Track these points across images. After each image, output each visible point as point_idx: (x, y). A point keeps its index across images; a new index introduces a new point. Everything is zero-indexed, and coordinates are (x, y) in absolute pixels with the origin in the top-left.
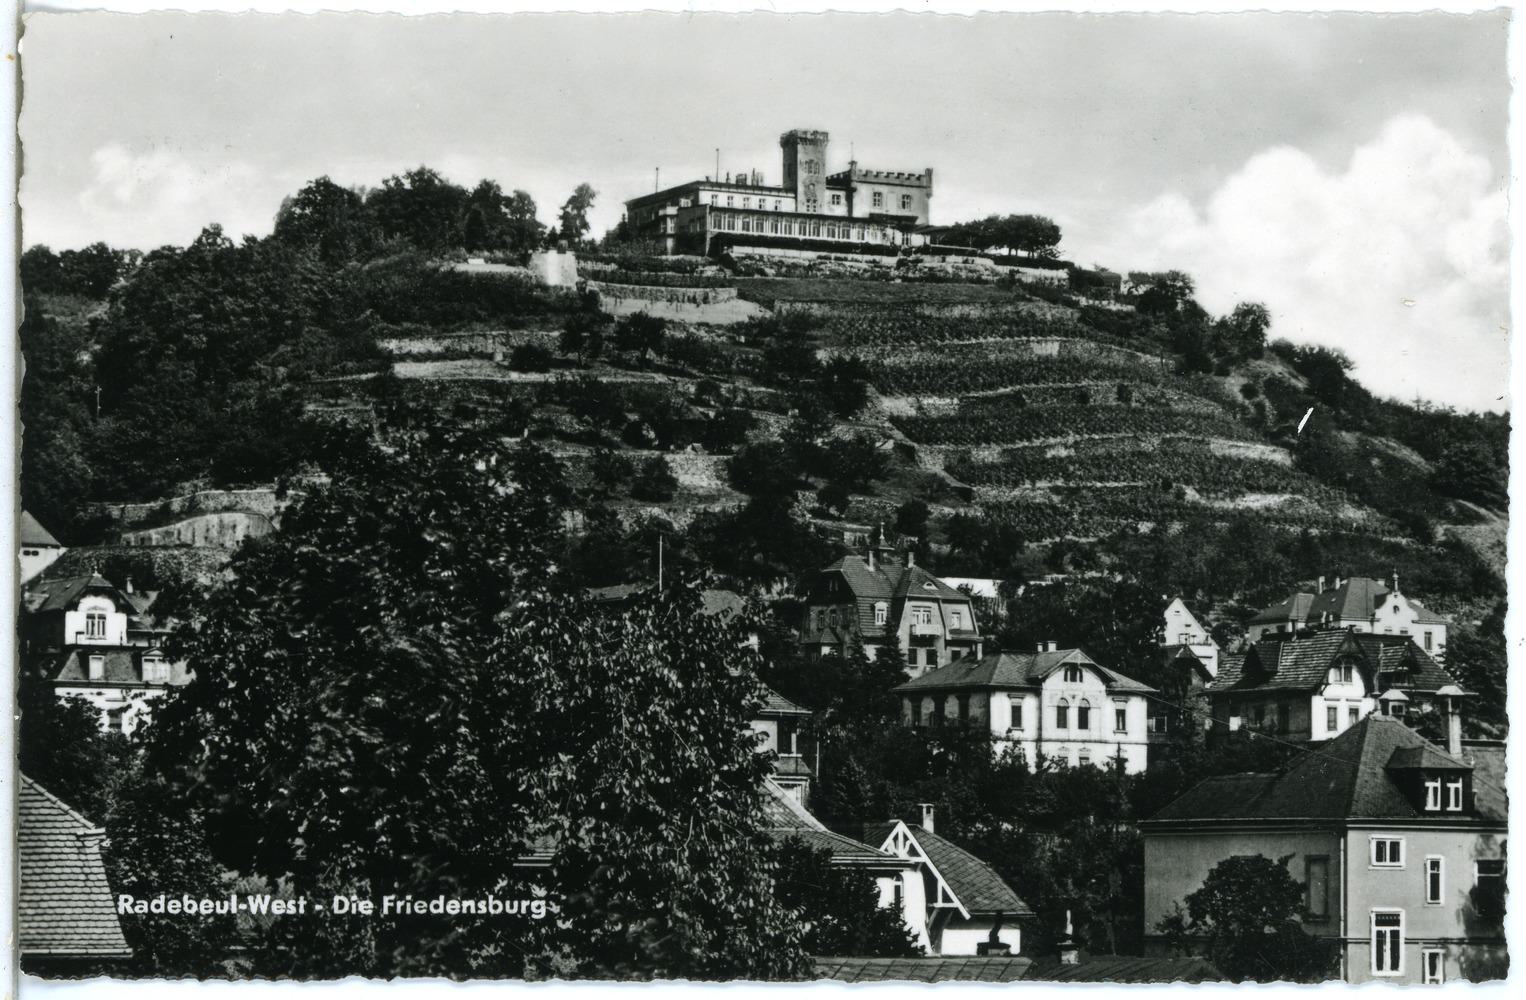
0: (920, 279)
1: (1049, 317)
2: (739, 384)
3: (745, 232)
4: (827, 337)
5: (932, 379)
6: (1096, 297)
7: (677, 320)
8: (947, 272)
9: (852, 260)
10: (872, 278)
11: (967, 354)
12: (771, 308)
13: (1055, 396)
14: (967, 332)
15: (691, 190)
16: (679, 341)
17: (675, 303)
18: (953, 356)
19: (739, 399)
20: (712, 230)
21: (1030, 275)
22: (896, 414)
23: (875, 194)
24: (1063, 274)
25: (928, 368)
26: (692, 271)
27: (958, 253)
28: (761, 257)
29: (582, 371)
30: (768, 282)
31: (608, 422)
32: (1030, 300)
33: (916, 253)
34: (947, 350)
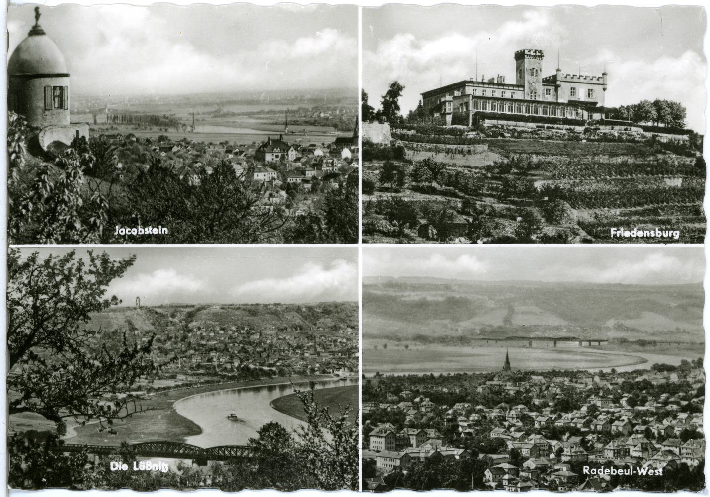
0: (598, 140)
1: (676, 163)
5: (604, 199)
8: (614, 136)
9: (558, 128)
10: (569, 140)
11: (625, 185)
12: (508, 157)
13: (679, 211)
14: (626, 172)
15: (461, 85)
17: (450, 154)
18: (617, 186)
19: (488, 211)
20: (472, 110)
21: (665, 138)
22: (581, 221)
23: (572, 89)
24: (686, 137)
25: (602, 193)
26: (461, 135)
28: (503, 126)
29: (393, 194)
30: (506, 141)
31: (408, 224)
32: (665, 153)
33: (595, 124)
34: (613, 183)
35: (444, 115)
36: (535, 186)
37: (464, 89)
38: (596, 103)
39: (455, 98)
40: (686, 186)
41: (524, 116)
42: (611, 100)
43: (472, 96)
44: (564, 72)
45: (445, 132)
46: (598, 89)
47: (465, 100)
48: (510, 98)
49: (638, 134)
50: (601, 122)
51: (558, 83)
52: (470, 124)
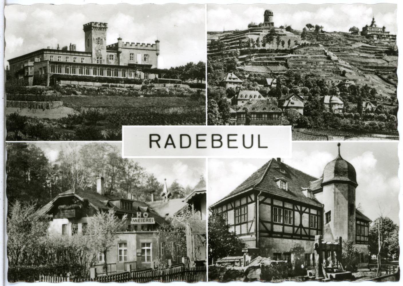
3: (66, 74)
4: (106, 124)
7: (33, 117)
8: (166, 92)
9: (120, 87)
10: (129, 95)
12: (79, 111)
15: (40, 53)
16: (33, 128)
17: (32, 110)
23: (131, 54)
26: (41, 93)
27: (172, 82)
28: (75, 85)
30: (78, 98)
33: (151, 82)
35: (27, 77)
36: (102, 134)
37: (43, 56)
38: (151, 66)
39: (35, 63)
43: (50, 62)
44: (125, 41)
45: (28, 91)
46: (152, 54)
47: (44, 65)
48: (80, 62)
49: (186, 90)
51: (120, 50)
52: (48, 84)
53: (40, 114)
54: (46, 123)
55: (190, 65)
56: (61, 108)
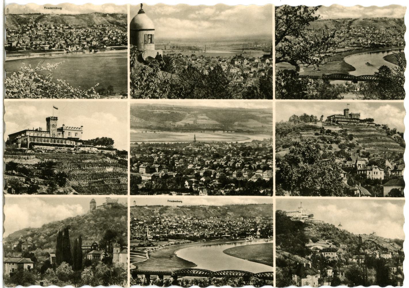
1: (111, 162)
2: (36, 179)
6: (122, 157)
10: (68, 153)
15: (25, 132)
19: (36, 182)
21: (106, 152)
24: (114, 152)
25: (81, 175)
26: (25, 151)
27: (89, 147)
35: (18, 144)
39: (22, 137)
40: (114, 171)
41: (50, 144)
42: (85, 137)
44: (66, 126)
46: (79, 133)
47: (26, 138)
50: (81, 146)
51: (64, 130)
53: (24, 162)
54: (27, 166)
55: (97, 139)
56: (34, 159)
